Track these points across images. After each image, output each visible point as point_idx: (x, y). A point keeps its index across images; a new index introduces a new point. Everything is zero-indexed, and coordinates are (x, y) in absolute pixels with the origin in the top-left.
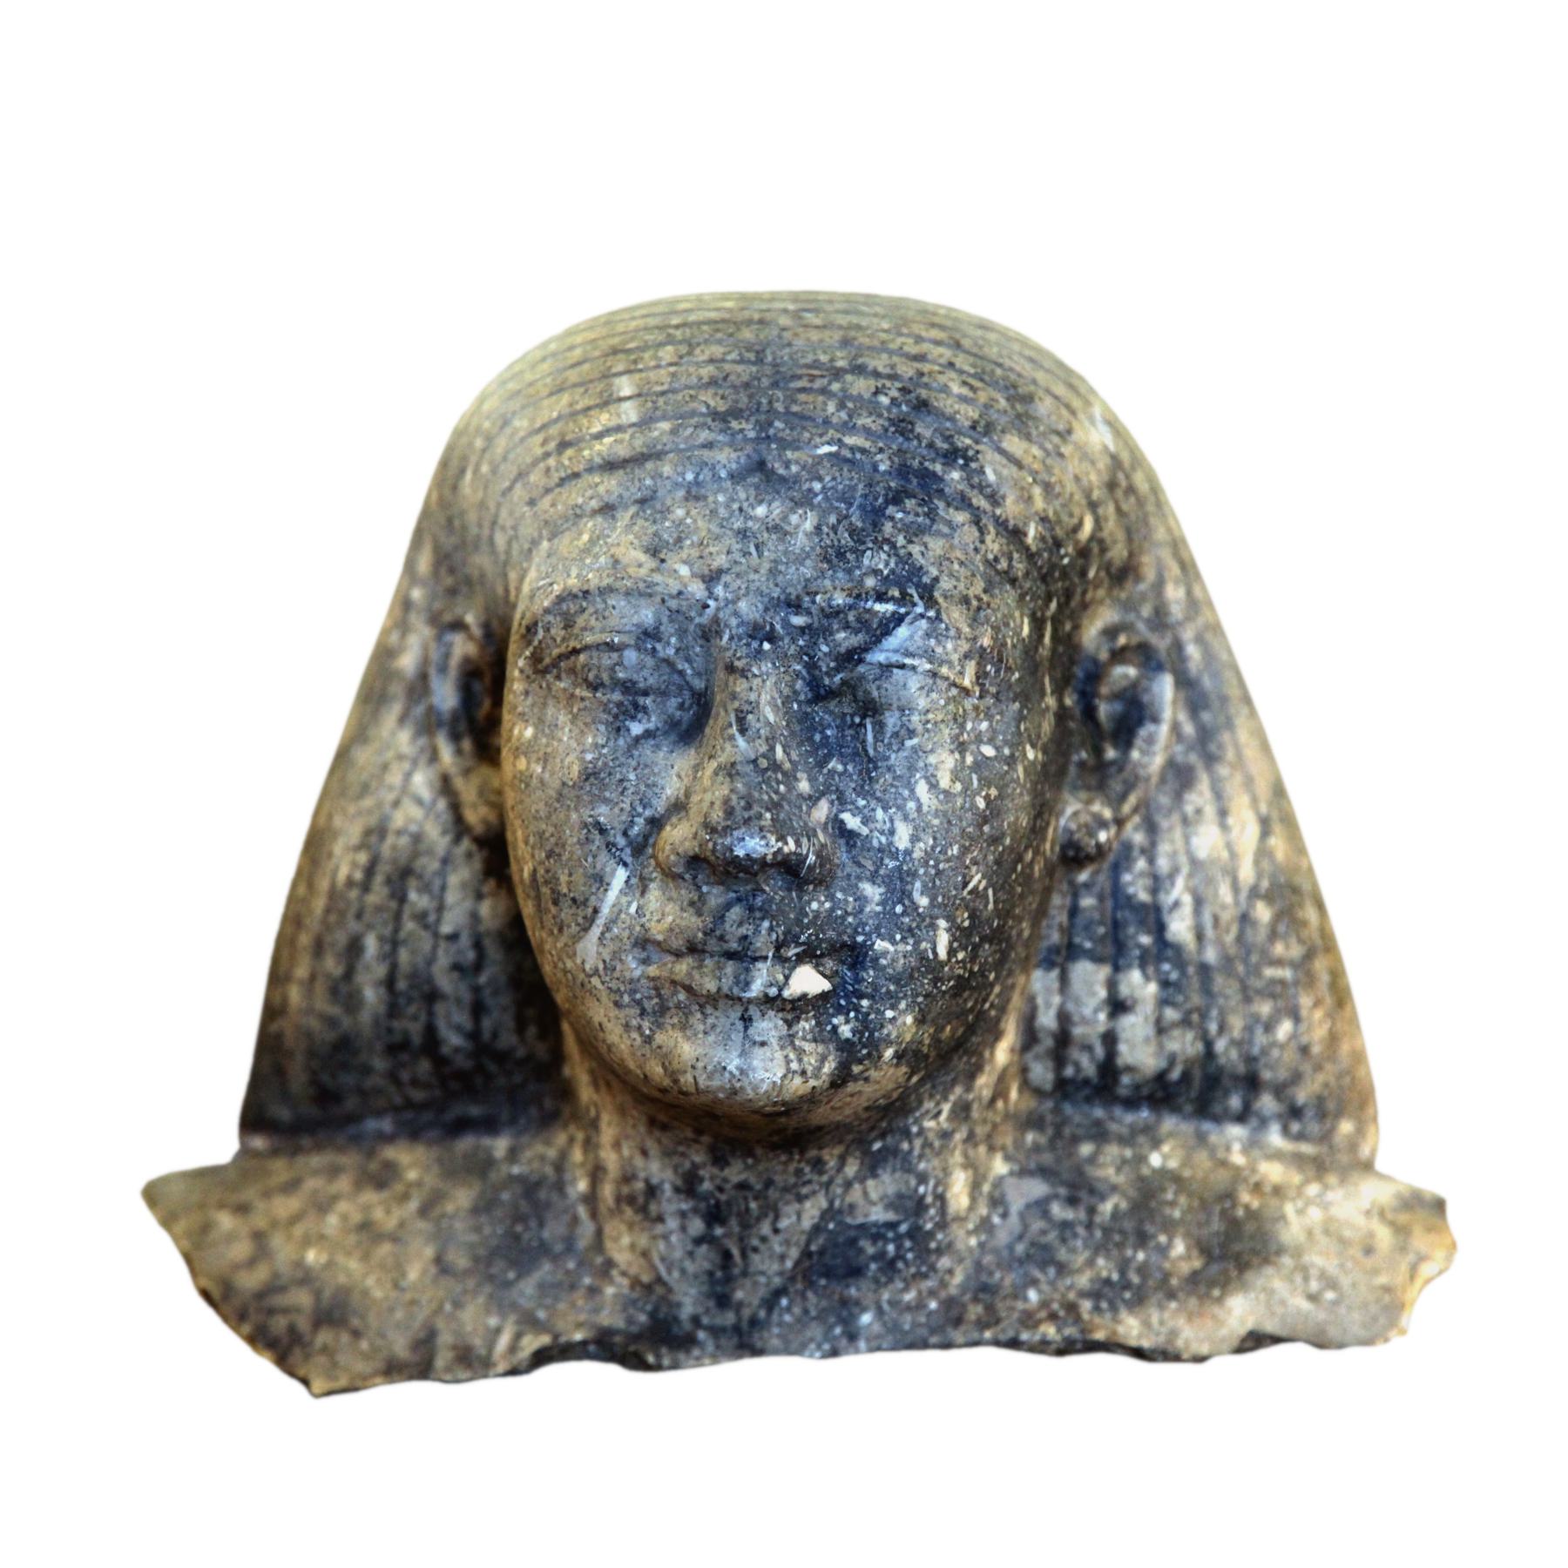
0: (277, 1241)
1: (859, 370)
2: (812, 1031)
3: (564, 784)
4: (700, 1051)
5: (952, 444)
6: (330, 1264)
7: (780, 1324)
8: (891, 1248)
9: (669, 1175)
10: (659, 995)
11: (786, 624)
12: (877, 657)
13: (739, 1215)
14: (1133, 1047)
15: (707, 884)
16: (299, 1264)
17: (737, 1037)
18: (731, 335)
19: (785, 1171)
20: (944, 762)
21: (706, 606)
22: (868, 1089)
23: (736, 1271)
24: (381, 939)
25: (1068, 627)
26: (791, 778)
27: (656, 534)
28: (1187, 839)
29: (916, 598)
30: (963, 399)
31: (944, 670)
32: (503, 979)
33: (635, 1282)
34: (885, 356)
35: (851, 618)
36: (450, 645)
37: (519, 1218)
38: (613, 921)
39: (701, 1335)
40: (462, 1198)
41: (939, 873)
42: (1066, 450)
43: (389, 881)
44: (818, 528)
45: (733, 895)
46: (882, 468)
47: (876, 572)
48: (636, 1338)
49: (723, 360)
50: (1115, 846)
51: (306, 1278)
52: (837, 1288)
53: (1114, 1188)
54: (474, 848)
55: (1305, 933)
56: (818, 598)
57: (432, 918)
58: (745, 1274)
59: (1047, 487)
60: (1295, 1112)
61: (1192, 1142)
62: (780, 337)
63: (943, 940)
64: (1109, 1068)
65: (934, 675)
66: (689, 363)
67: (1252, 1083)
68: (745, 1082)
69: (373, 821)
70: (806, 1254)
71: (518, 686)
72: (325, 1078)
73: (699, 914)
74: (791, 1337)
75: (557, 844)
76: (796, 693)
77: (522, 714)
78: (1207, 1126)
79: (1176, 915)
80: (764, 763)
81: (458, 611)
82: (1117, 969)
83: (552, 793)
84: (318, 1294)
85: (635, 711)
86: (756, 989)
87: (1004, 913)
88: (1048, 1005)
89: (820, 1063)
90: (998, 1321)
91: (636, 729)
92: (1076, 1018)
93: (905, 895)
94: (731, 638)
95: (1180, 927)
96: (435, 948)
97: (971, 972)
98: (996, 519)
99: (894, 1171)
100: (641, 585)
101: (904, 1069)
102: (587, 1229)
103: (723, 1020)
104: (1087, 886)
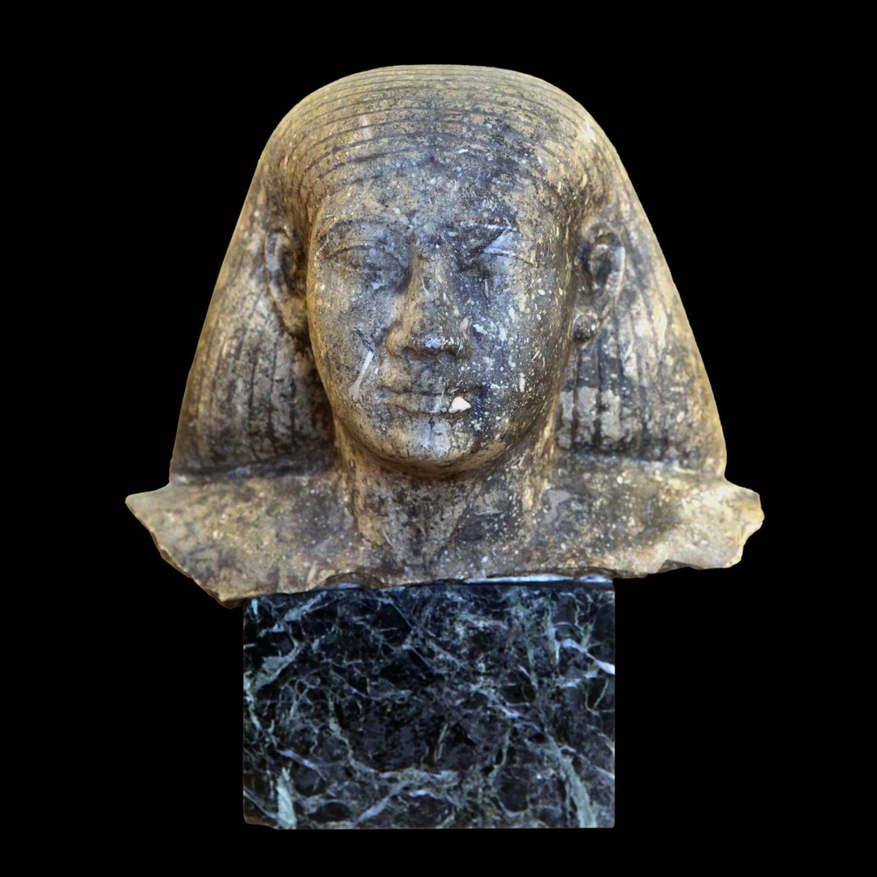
0: (198, 527)
1: (476, 111)
2: (462, 427)
3: (341, 312)
4: (410, 438)
5: (521, 146)
6: (224, 538)
7: (444, 563)
8: (496, 526)
9: (391, 494)
10: (389, 412)
11: (446, 236)
12: (490, 250)
13: (424, 512)
14: (609, 427)
16: (210, 538)
17: (428, 431)
18: (414, 94)
19: (446, 492)
20: (522, 299)
22: (488, 453)
23: (423, 538)
24: (245, 382)
25: (576, 228)
26: (450, 309)
27: (383, 193)
28: (633, 328)
29: (508, 222)
30: (526, 124)
31: (521, 256)
32: (305, 400)
33: (374, 544)
34: (488, 104)
35: (477, 232)
36: (275, 239)
37: (316, 515)
39: (406, 569)
40: (287, 505)
41: (520, 352)
42: (574, 145)
43: (248, 354)
44: (460, 189)
45: (424, 365)
46: (490, 159)
47: (488, 210)
49: (411, 107)
50: (599, 331)
51: (213, 545)
52: (471, 546)
53: (601, 494)
54: (290, 338)
55: (689, 370)
56: (462, 223)
57: (270, 372)
58: (427, 540)
59: (566, 164)
60: (686, 455)
61: (636, 470)
62: (438, 95)
63: (522, 382)
64: (597, 437)
65: (517, 258)
66: (396, 109)
67: (665, 442)
68: (432, 453)
69: (239, 325)
70: (456, 530)
71: (316, 265)
72: (217, 448)
73: (409, 374)
74: (450, 569)
76: (451, 268)
77: (319, 279)
78: (644, 463)
79: (628, 364)
80: (438, 303)
81: (280, 223)
82: (601, 390)
83: (336, 317)
84: (220, 552)
85: (375, 277)
86: (437, 409)
87: (550, 368)
88: (568, 409)
89: (466, 442)
90: (547, 559)
91: (376, 286)
92: (581, 414)
93: (504, 362)
94: (421, 243)
95: (630, 370)
96: (272, 386)
97: (535, 397)
98: (543, 181)
99: (498, 489)
100: (377, 218)
101: (504, 443)
102: (349, 519)
103: (420, 423)
104: (585, 351)
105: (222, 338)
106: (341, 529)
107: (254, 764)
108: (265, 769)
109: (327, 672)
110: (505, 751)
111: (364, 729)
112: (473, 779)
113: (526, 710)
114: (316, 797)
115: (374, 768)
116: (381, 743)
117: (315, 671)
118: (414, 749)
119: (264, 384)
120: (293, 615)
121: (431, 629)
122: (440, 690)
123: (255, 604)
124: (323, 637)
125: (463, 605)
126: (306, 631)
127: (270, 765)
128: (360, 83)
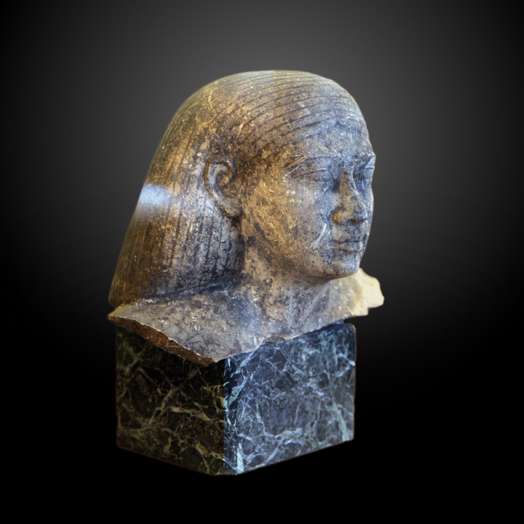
3: (310, 205)
12: (367, 167)
15: (349, 225)
17: (353, 260)
21: (341, 159)
23: (301, 314)
24: (205, 245)
32: (235, 251)
38: (324, 237)
39: (292, 331)
48: (280, 334)
54: (228, 219)
57: (219, 238)
58: (302, 314)
73: (349, 233)
75: (308, 219)
84: (203, 336)
94: (346, 166)
96: (220, 245)
105: (188, 223)
106: (256, 315)
107: (228, 444)
108: (232, 445)
109: (255, 390)
110: (319, 413)
111: (269, 415)
114: (251, 455)
115: (272, 434)
117: (251, 390)
118: (287, 421)
119: (216, 245)
120: (243, 364)
121: (294, 359)
122: (296, 389)
123: (229, 361)
124: (255, 372)
125: (305, 344)
127: (235, 443)
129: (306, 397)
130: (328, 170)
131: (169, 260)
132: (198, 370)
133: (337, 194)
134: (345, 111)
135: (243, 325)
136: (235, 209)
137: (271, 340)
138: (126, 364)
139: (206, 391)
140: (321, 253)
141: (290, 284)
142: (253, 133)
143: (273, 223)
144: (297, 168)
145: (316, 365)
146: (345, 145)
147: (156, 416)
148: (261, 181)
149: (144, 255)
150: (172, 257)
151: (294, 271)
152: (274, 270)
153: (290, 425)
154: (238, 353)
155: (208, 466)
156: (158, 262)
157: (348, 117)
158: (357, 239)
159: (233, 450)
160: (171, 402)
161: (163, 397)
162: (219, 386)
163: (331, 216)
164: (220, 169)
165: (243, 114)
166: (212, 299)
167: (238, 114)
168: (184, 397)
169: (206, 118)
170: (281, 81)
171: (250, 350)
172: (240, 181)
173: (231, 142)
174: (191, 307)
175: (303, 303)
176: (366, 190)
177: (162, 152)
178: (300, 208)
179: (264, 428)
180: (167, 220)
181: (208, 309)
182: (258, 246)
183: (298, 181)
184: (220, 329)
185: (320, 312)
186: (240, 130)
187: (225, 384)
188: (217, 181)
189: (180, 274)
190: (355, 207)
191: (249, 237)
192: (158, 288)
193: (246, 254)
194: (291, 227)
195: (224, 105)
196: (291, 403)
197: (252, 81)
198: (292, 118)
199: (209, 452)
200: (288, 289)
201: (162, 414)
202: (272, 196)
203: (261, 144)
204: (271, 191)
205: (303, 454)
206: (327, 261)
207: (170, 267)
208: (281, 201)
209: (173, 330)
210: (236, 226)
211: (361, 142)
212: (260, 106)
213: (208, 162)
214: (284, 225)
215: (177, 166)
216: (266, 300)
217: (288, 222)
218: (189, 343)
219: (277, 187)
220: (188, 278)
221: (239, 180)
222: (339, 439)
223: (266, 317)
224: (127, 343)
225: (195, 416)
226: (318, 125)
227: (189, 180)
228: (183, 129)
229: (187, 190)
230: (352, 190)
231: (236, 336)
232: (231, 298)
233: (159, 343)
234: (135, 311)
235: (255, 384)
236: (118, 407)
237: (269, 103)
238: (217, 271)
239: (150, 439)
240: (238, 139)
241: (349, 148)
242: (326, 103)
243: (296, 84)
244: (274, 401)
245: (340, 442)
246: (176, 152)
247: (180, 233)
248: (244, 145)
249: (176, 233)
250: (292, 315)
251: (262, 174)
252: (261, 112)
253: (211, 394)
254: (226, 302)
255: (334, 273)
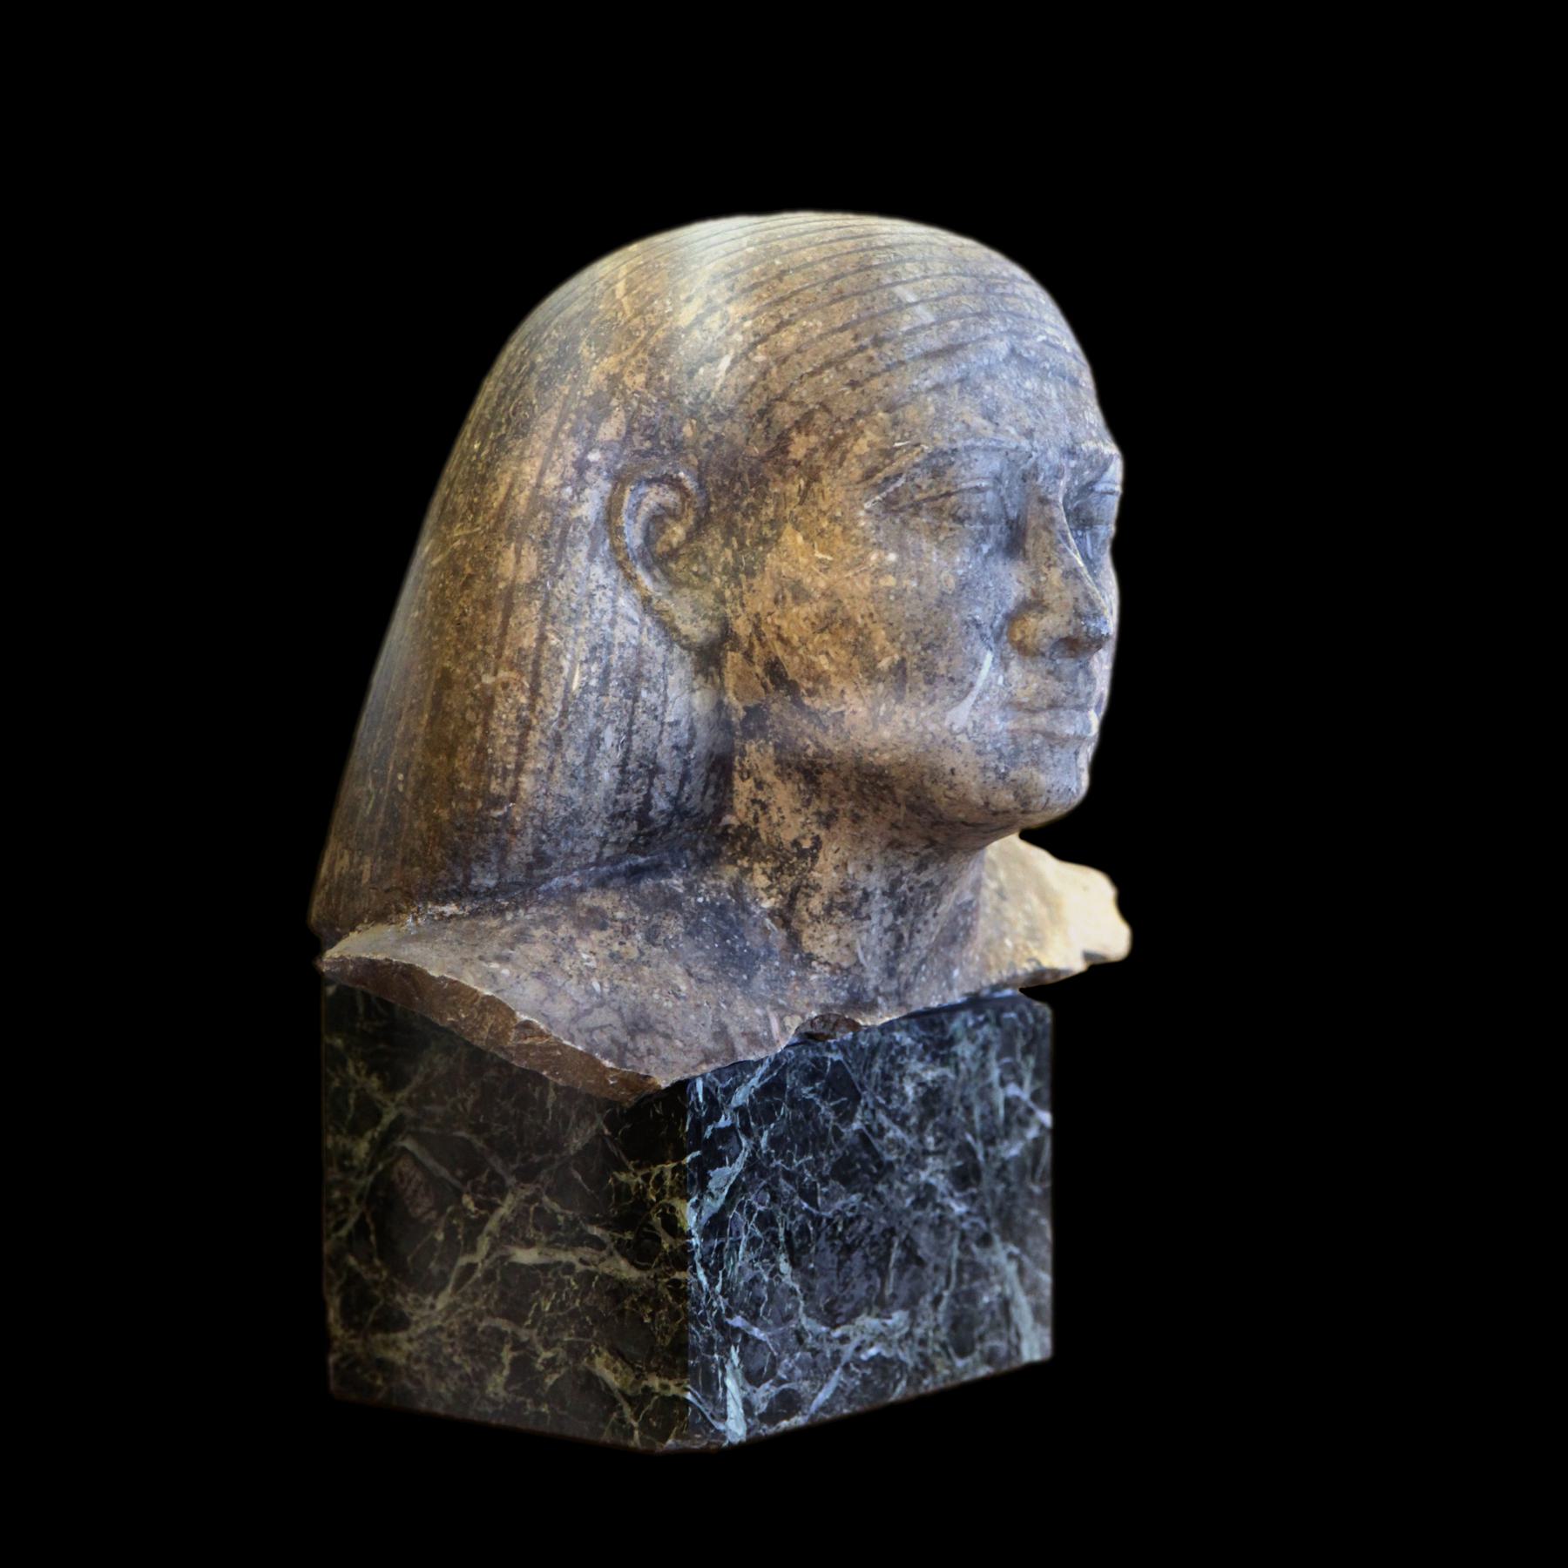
3: (943, 593)
12: (1100, 487)
21: (1031, 456)
24: (617, 730)
32: (704, 751)
38: (985, 691)
39: (880, 1000)
48: (846, 1007)
54: (685, 653)
57: (660, 710)
58: (908, 951)
73: (1059, 680)
75: (937, 639)
94: (1045, 479)
96: (661, 733)
105: (565, 663)
106: (770, 952)
109: (775, 1182)
110: (954, 1266)
112: (923, 1318)
113: (973, 1197)
114: (767, 1385)
115: (826, 1324)
116: (832, 1283)
117: (764, 1182)
118: (866, 1286)
119: (650, 731)
120: (741, 1097)
121: (880, 1094)
122: (891, 1187)
123: (700, 1084)
124: (772, 1125)
125: (912, 1049)
126: (754, 1121)
128: (713, 240)
129: (919, 1213)
130: (994, 489)
131: (511, 779)
132: (600, 1121)
133: (1021, 563)
134: (1031, 318)
135: (734, 980)
136: (707, 622)
137: (819, 1029)
138: (356, 1131)
139: (628, 1186)
140: (976, 742)
141: (876, 850)
142: (762, 383)
143: (827, 654)
144: (901, 481)
145: (943, 1115)
146: (1037, 417)
147: (457, 1287)
148: (789, 528)
149: (428, 767)
150: (519, 769)
151: (890, 806)
152: (825, 808)
153: (874, 1299)
154: (726, 1061)
155: (635, 1424)
156: (476, 787)
157: (1041, 338)
158: (1083, 700)
159: (713, 1366)
160: (510, 1232)
161: (484, 1220)
162: (671, 1165)
163: (1005, 630)
164: (658, 499)
165: (729, 325)
166: (638, 903)
167: (715, 326)
168: (555, 1214)
169: (612, 345)
170: (836, 231)
171: (761, 1054)
172: (718, 536)
173: (693, 415)
174: (575, 926)
175: (911, 916)
176: (1099, 560)
177: (474, 458)
178: (913, 602)
179: (802, 1302)
180: (499, 656)
181: (627, 932)
182: (776, 734)
183: (905, 523)
184: (670, 989)
185: (956, 948)
186: (722, 373)
187: (688, 1159)
188: (648, 540)
189: (543, 821)
190: (1076, 599)
191: (746, 709)
192: (477, 868)
193: (736, 764)
194: (884, 664)
195: (668, 302)
196: (876, 1231)
197: (747, 235)
198: (882, 334)
199: (640, 1377)
200: (869, 868)
201: (478, 1274)
202: (825, 571)
203: (785, 414)
204: (819, 555)
205: (912, 1393)
206: (996, 769)
207: (513, 799)
208: (853, 584)
209: (527, 991)
210: (707, 675)
211: (1083, 412)
212: (782, 300)
213: (619, 480)
214: (863, 659)
215: (527, 492)
216: (799, 905)
217: (877, 648)
218: (579, 1030)
219: (840, 544)
220: (567, 836)
221: (716, 533)
222: (1013, 1353)
223: (801, 958)
224: (361, 1064)
225: (592, 1268)
226: (960, 353)
227: (564, 532)
228: (540, 384)
229: (558, 564)
230: (1065, 551)
231: (718, 1010)
232: (693, 900)
233: (484, 1034)
234: (408, 939)
235: (773, 1165)
236: (329, 1270)
237: (807, 291)
238: (652, 813)
239: (441, 1361)
240: (714, 404)
241: (1051, 425)
242: (976, 292)
243: (882, 240)
244: (829, 1221)
245: (1015, 1364)
246: (522, 453)
247: (541, 695)
248: (734, 422)
249: (528, 694)
250: (878, 951)
251: (793, 508)
252: (786, 317)
253: (645, 1192)
254: (681, 910)
255: (1016, 805)
